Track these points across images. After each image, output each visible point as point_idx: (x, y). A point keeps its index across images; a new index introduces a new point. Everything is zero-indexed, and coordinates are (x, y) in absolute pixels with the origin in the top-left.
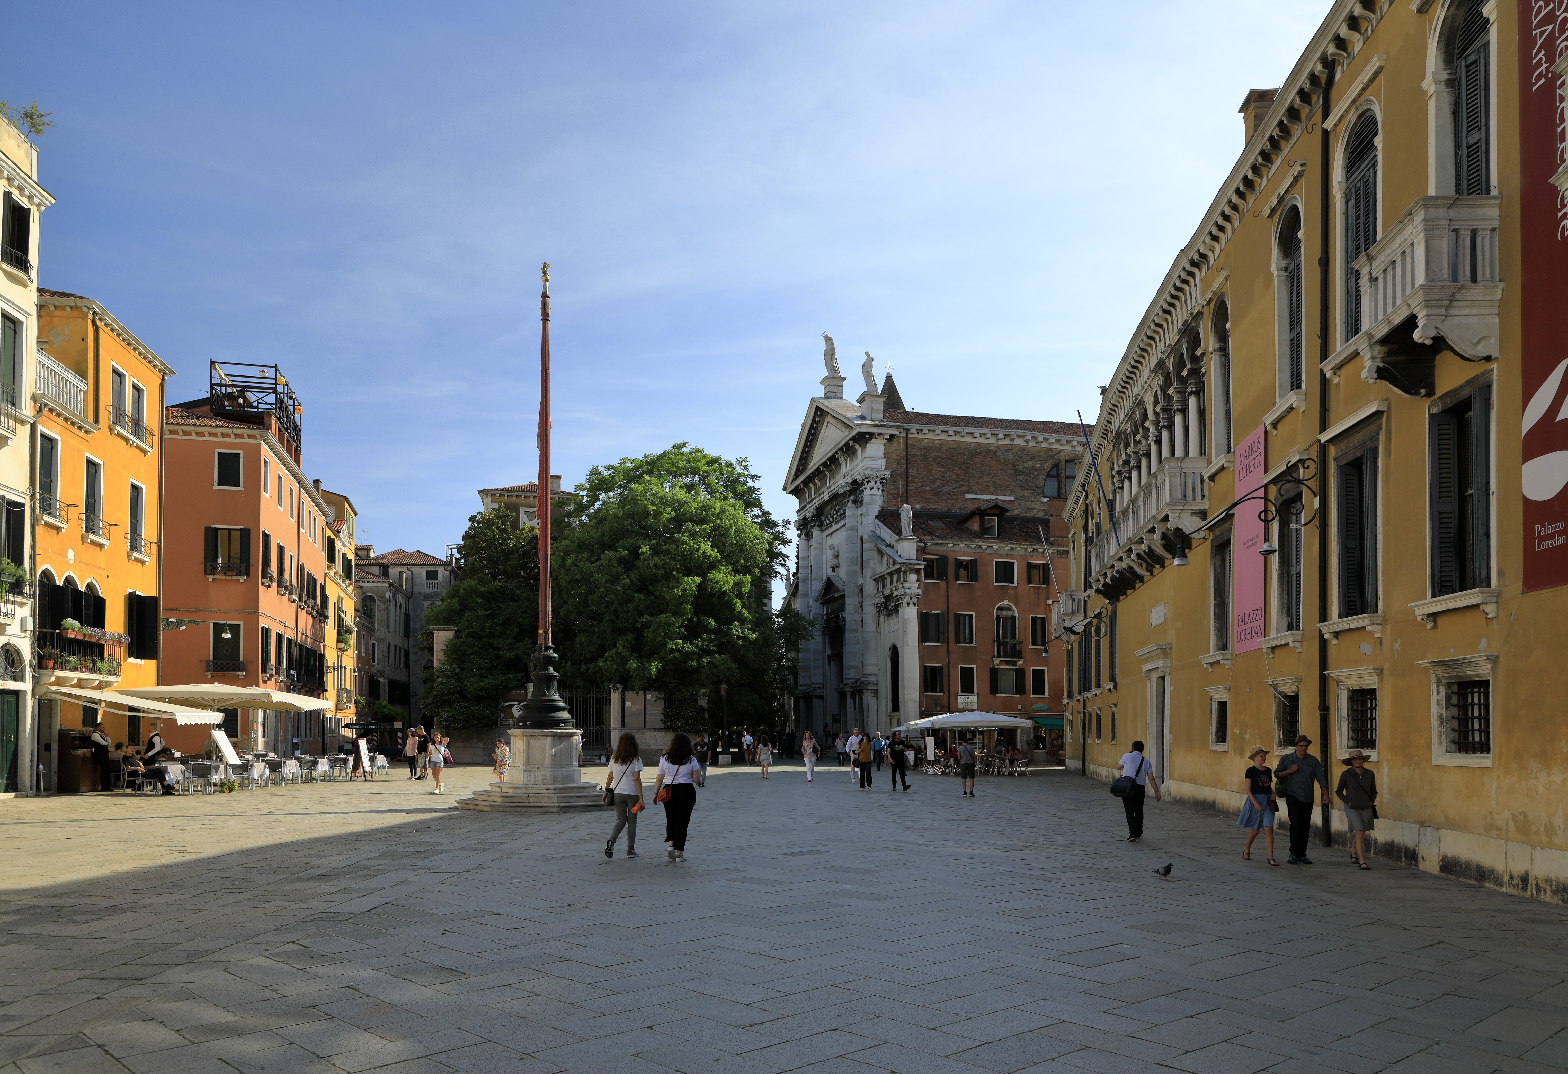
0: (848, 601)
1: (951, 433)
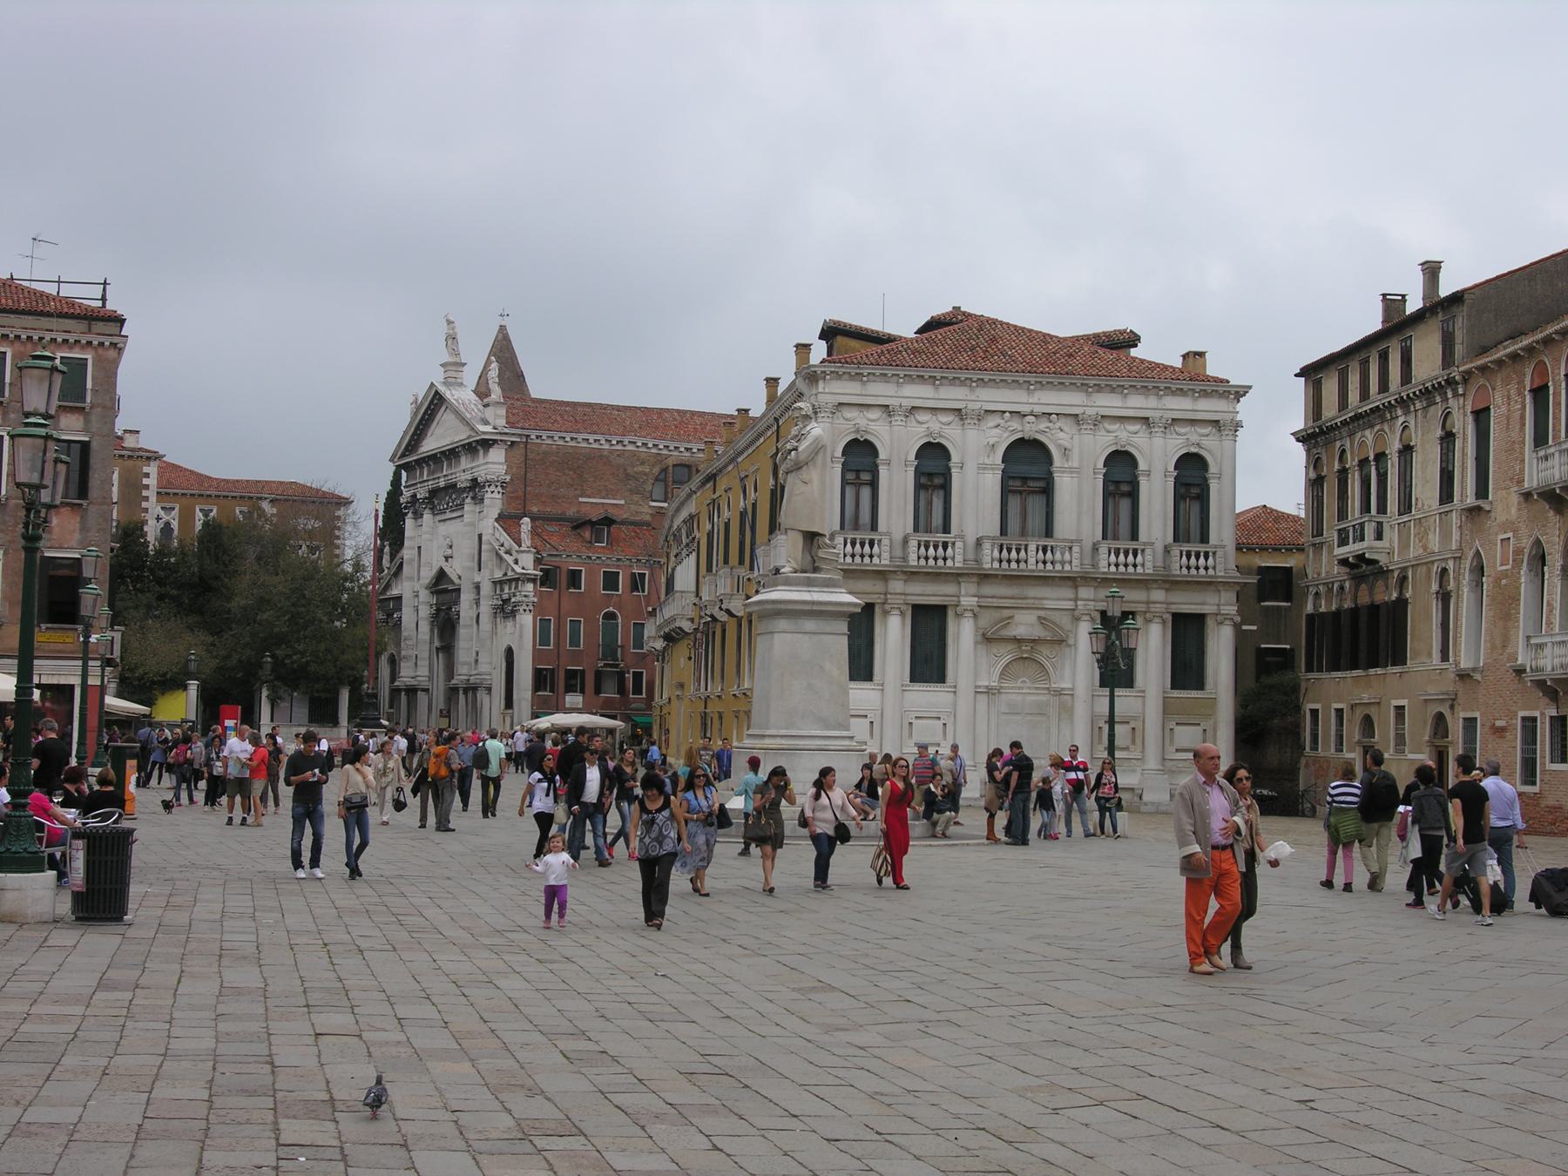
0: (463, 596)
1: (568, 439)
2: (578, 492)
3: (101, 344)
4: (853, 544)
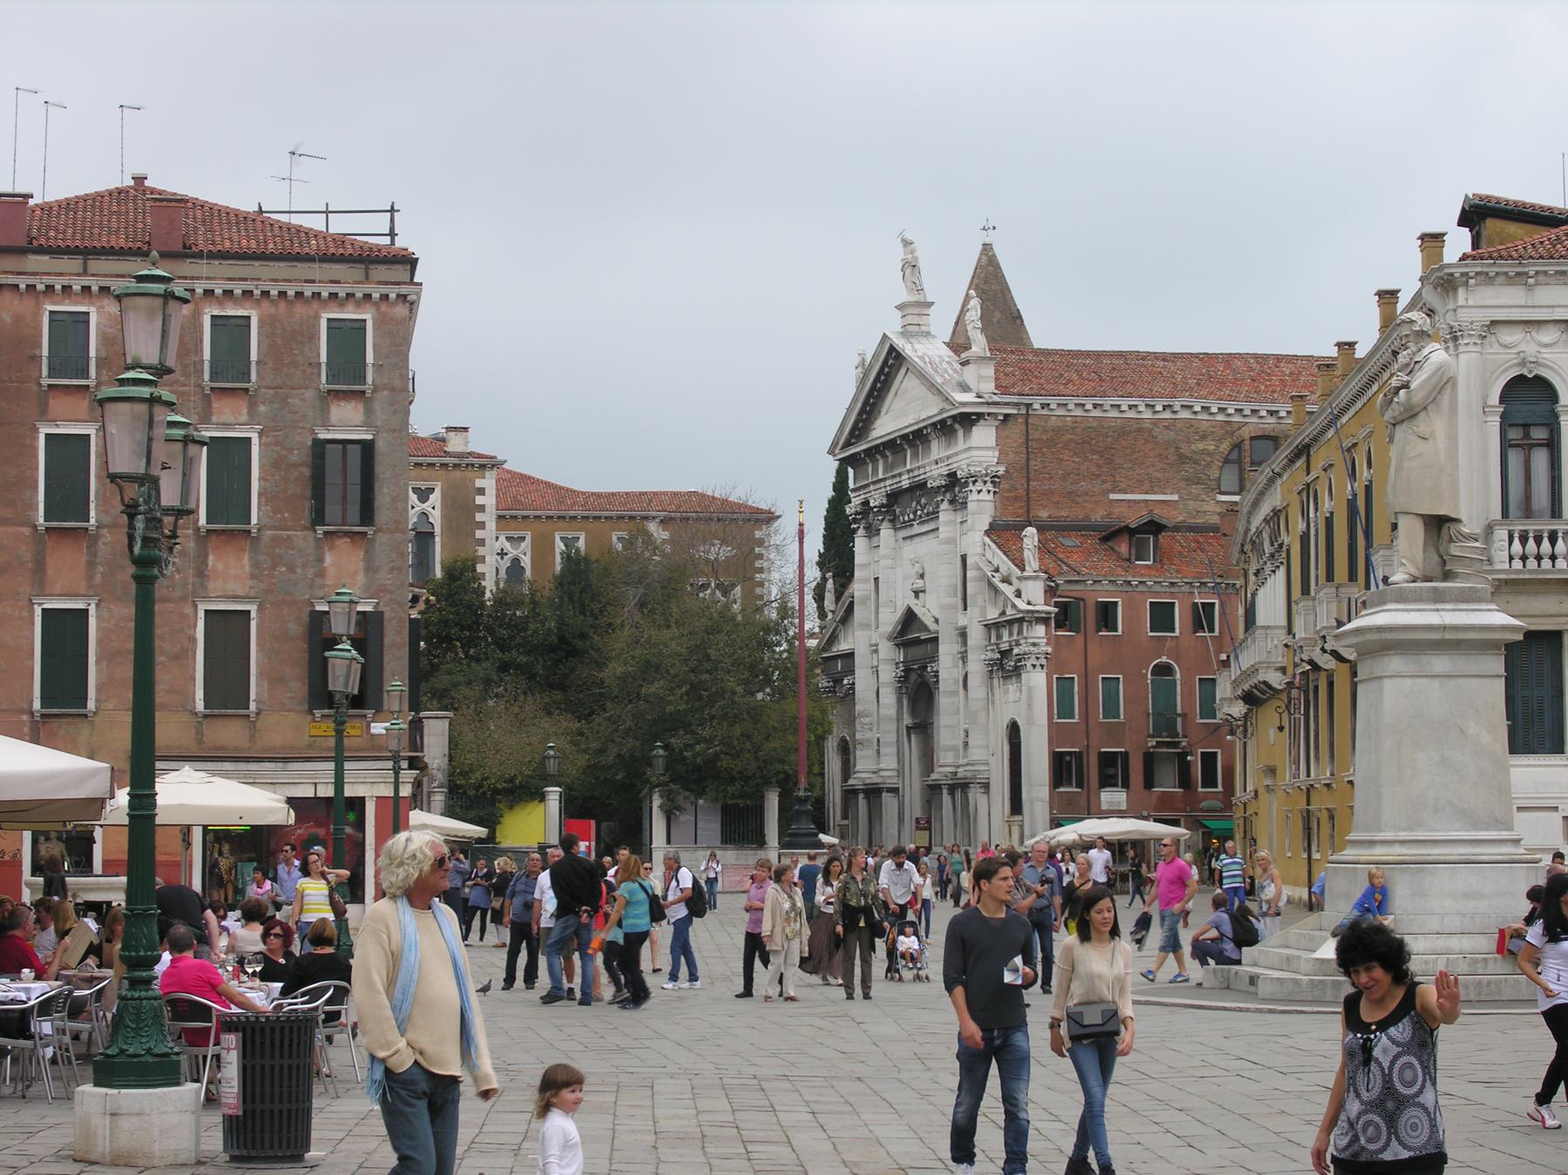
0: (943, 649)
1: (1089, 407)
2: (1108, 486)
3: (385, 297)
4: (1524, 540)
